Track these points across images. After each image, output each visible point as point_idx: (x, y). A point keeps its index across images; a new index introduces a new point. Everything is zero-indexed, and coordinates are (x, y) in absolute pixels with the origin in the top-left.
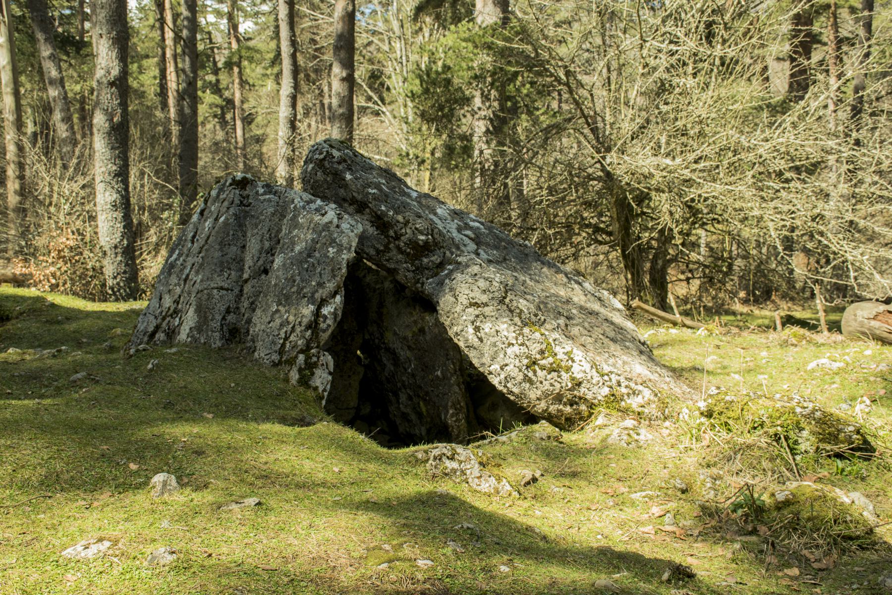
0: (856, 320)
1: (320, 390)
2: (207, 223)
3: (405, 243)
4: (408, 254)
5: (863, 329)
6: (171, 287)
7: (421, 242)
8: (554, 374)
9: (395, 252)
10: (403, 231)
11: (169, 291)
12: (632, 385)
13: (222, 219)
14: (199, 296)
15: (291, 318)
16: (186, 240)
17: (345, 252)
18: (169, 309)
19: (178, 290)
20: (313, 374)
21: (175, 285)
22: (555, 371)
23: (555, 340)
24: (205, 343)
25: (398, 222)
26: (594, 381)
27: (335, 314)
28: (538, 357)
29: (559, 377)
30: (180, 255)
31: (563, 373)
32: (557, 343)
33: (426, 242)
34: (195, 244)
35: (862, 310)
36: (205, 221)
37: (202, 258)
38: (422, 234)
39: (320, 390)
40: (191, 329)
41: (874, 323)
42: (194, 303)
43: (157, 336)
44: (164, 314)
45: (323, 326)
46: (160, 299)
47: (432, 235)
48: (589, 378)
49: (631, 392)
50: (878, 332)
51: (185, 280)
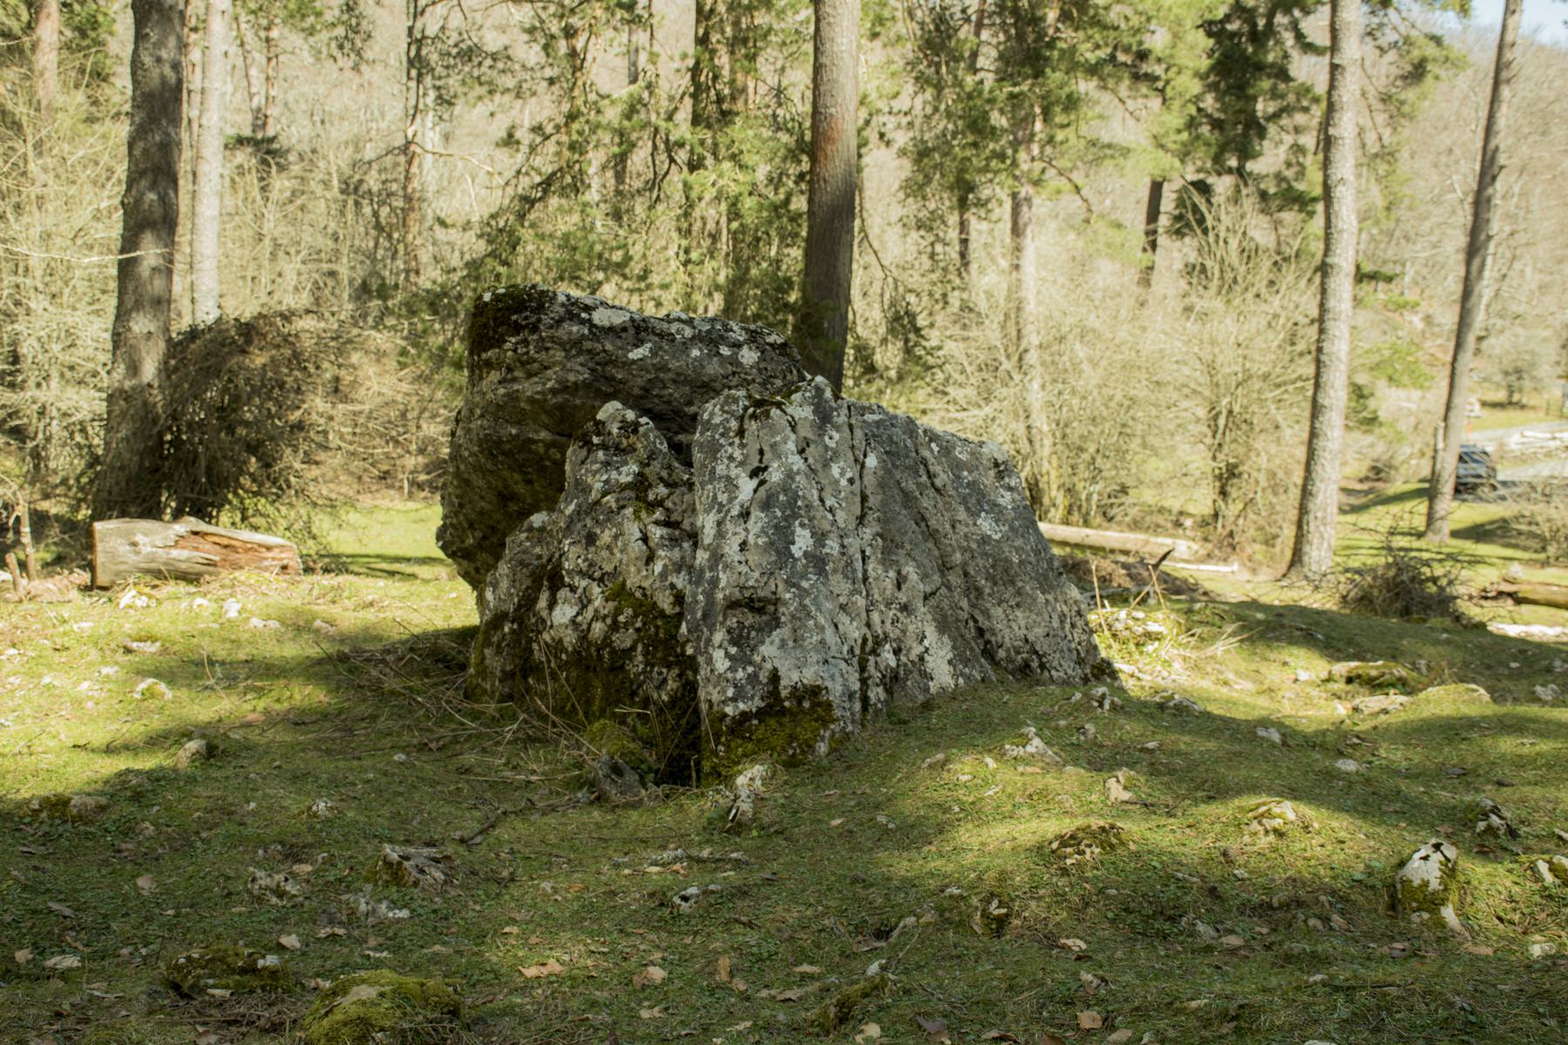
0: (138, 553)
2: (835, 470)
5: (154, 566)
6: (842, 600)
11: (843, 607)
13: (872, 461)
14: (933, 602)
15: (1065, 609)
16: (808, 507)
18: (865, 640)
19: (861, 602)
21: (852, 593)
24: (983, 680)
30: (820, 538)
34: (841, 516)
35: (145, 535)
36: (826, 465)
37: (881, 536)
40: (950, 662)
41: (175, 553)
42: (929, 617)
43: (872, 695)
44: (857, 651)
46: (836, 626)
50: (183, 566)
51: (865, 579)
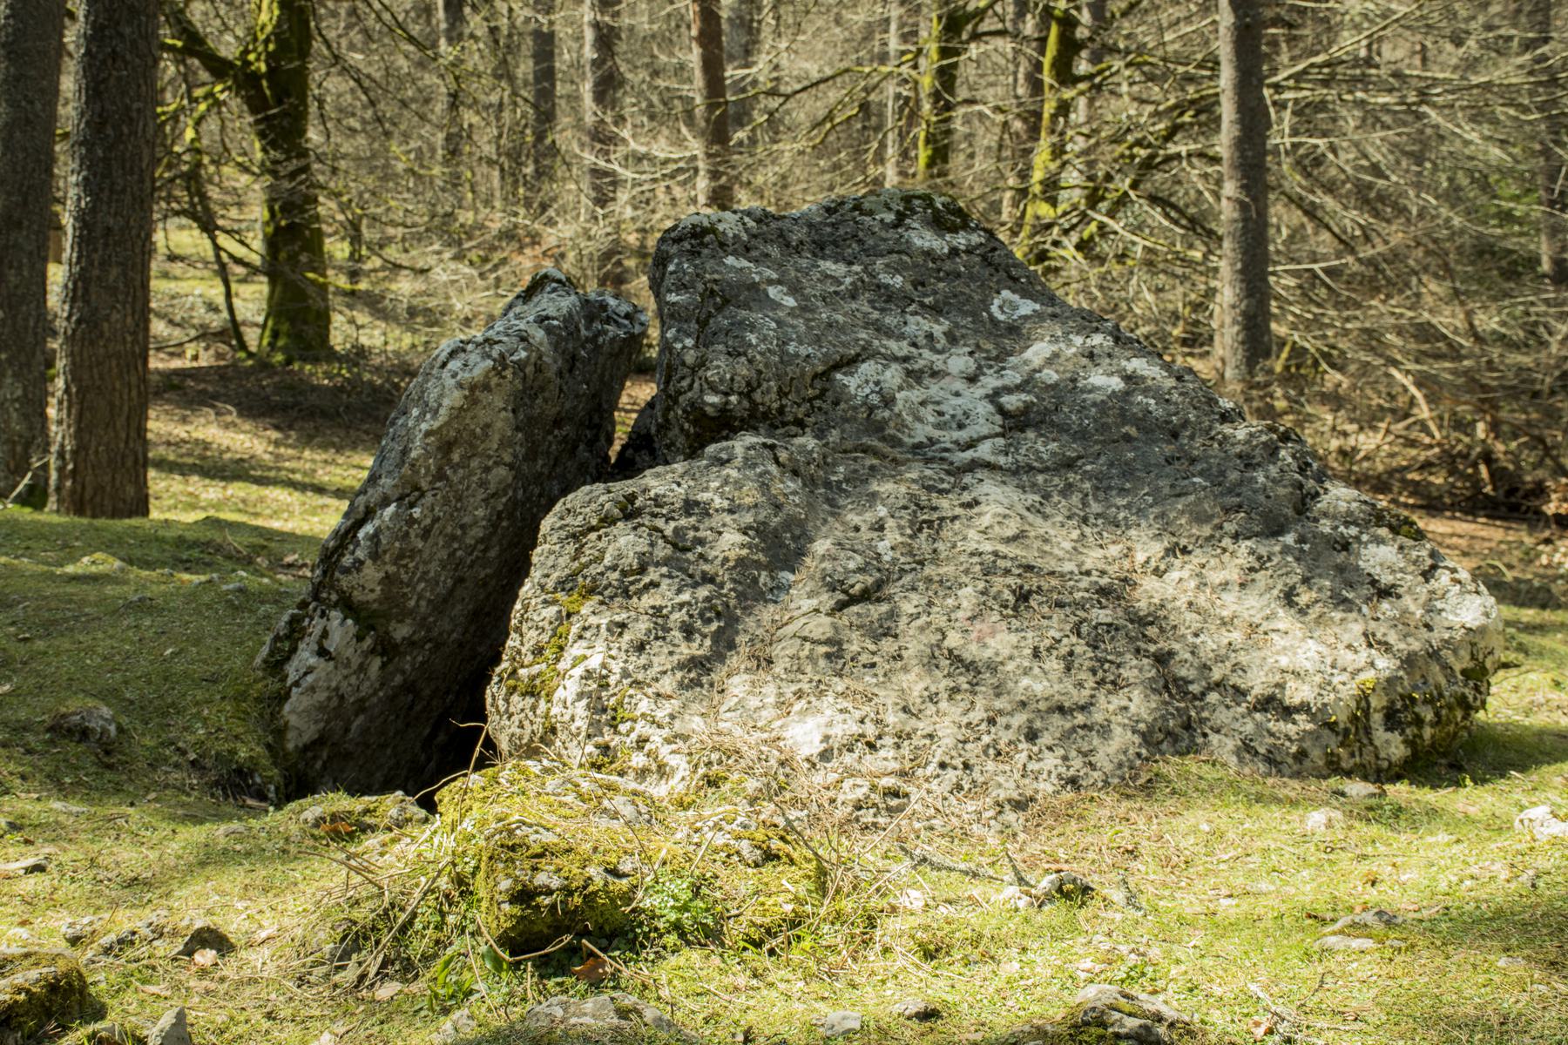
1: (289, 682)
3: (685, 411)
4: (687, 435)
7: (708, 409)
8: (530, 701)
9: (676, 431)
10: (685, 383)
12: (665, 751)
17: (428, 416)
20: (294, 650)
22: (532, 694)
23: (585, 629)
25: (684, 364)
26: (573, 728)
27: (375, 537)
28: (529, 658)
29: (534, 708)
31: (542, 703)
32: (588, 634)
33: (724, 410)
38: (714, 389)
39: (289, 682)
45: (347, 560)
47: (747, 394)
48: (567, 718)
49: (654, 767)
